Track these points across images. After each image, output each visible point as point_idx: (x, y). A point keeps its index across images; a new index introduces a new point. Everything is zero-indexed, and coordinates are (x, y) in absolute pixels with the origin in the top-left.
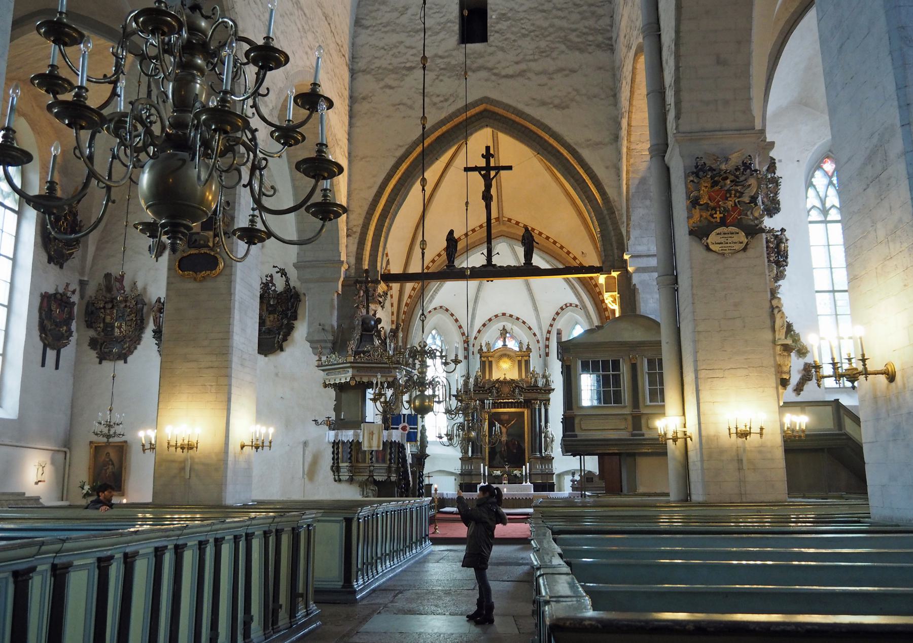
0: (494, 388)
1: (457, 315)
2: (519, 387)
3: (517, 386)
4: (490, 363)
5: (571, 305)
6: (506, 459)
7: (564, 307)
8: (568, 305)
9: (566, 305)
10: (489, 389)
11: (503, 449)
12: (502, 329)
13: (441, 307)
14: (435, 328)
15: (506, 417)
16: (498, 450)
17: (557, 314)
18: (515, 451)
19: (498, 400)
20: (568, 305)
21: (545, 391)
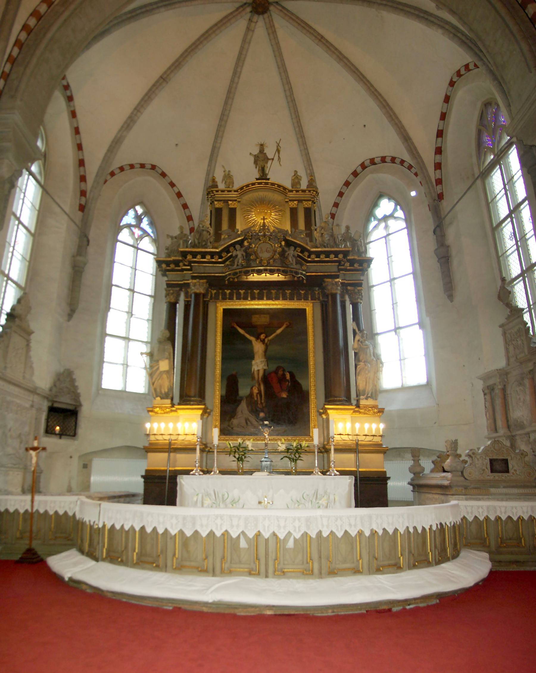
0: (238, 247)
1: (180, 187)
2: (296, 245)
3: (289, 244)
4: (233, 212)
5: (372, 162)
6: (262, 415)
7: (359, 169)
8: (367, 163)
9: (363, 166)
10: (227, 250)
11: (255, 391)
12: (256, 151)
13: (153, 167)
14: (141, 203)
15: (263, 320)
16: (243, 391)
17: (347, 184)
18: (284, 395)
19: (247, 273)
20: (367, 163)
21: (352, 262)
